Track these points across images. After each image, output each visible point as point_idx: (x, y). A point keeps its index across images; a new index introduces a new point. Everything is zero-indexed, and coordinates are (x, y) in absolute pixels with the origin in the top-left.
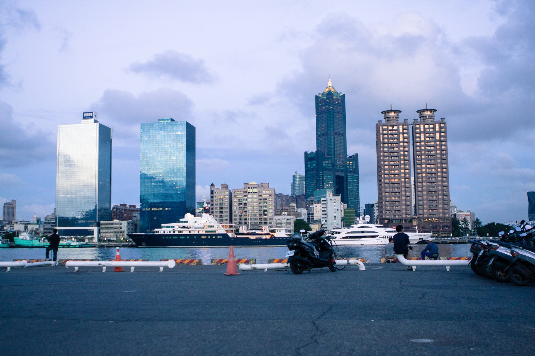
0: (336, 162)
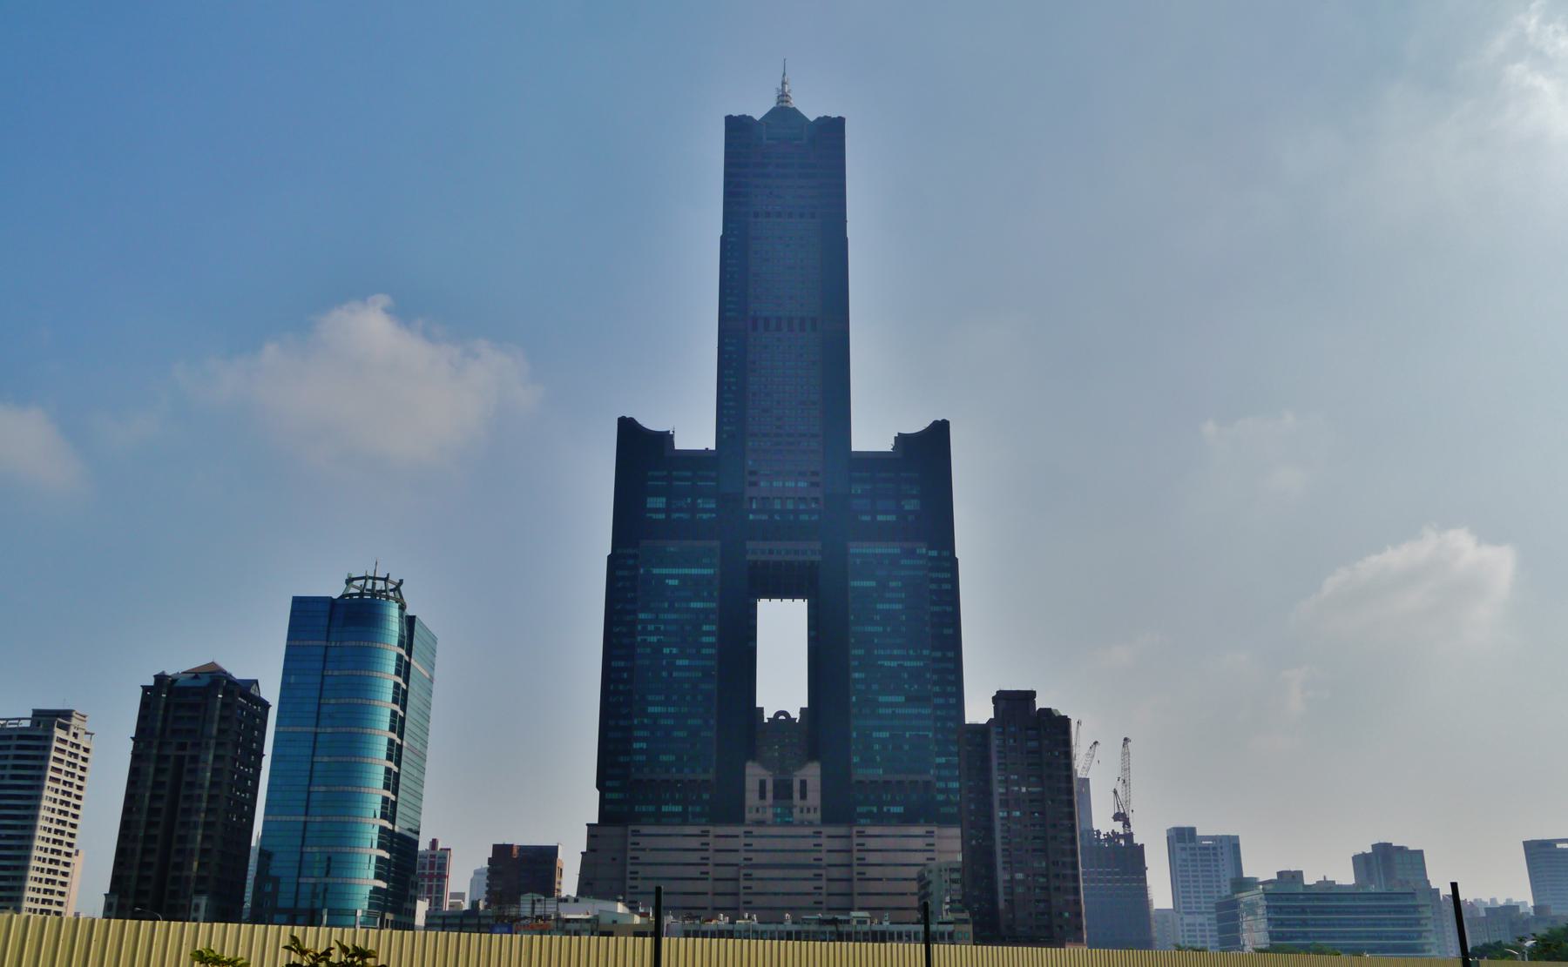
0: (755, 484)
